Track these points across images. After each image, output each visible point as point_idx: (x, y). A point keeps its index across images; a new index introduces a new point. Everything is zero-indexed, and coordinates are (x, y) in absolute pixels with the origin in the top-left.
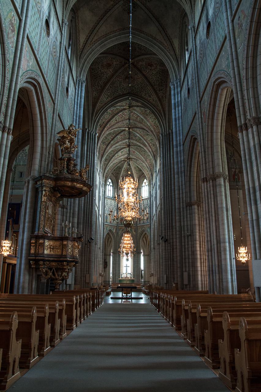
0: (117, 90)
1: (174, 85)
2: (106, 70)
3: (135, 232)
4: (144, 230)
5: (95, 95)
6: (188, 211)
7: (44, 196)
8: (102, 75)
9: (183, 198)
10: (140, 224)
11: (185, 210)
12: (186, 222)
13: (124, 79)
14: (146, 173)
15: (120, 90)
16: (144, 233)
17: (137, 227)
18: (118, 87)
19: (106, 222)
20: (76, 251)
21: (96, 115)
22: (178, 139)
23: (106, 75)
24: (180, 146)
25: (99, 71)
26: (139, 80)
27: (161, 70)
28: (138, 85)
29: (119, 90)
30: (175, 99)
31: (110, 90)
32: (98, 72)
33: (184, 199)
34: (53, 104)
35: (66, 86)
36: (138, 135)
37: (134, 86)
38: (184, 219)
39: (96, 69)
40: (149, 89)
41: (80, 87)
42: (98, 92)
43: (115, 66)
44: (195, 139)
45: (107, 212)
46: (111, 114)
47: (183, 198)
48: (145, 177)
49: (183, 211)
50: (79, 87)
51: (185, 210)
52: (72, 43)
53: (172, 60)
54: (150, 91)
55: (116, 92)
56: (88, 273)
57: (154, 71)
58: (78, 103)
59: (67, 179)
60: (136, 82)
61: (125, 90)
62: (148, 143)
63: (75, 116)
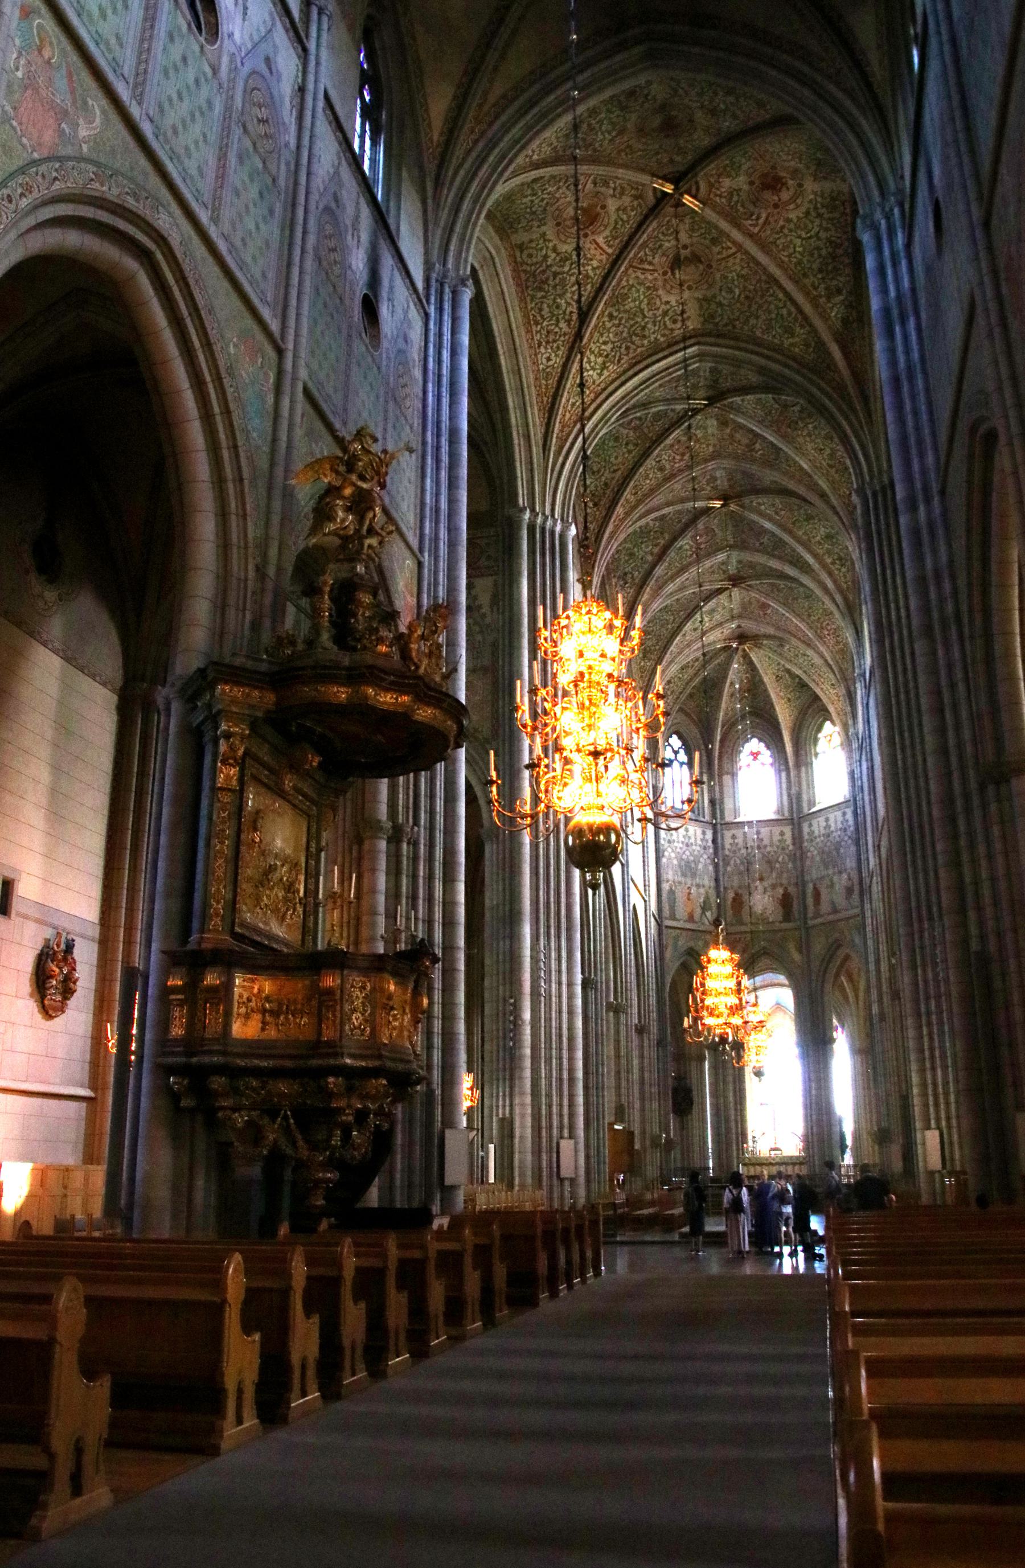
0: (644, 328)
1: (875, 227)
3: (800, 952)
4: (837, 940)
5: (549, 359)
6: (993, 807)
7: (224, 762)
8: (566, 269)
9: (960, 746)
10: (817, 915)
11: (976, 801)
12: (984, 863)
13: (665, 273)
14: (830, 694)
15: (654, 323)
16: (841, 953)
17: (807, 929)
18: (642, 311)
19: (673, 917)
20: (395, 1019)
21: (561, 448)
22: (916, 466)
24: (928, 501)
25: (550, 253)
26: (730, 264)
27: (822, 196)
28: (730, 291)
29: (649, 326)
30: (884, 291)
31: (609, 331)
32: (546, 257)
33: (969, 749)
34: (272, 354)
35: (361, 289)
36: (768, 525)
37: (714, 296)
38: (972, 846)
41: (447, 306)
42: (558, 348)
43: (613, 217)
44: (991, 437)
45: (671, 873)
46: (636, 445)
47: (960, 746)
48: (827, 716)
49: (968, 811)
50: (440, 310)
51: (976, 801)
52: (390, 117)
53: (855, 111)
55: (637, 335)
56: (571, 1137)
57: (792, 206)
58: (440, 376)
59: (328, 674)
60: (718, 276)
61: (675, 322)
62: (815, 556)
63: (429, 434)
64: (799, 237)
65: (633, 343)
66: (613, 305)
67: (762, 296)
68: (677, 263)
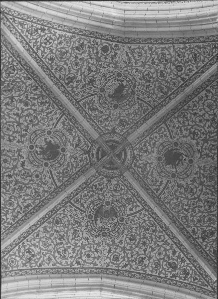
0: (65, 250)
2: (39, 170)
13: (90, 217)
23: (38, 184)
29: (70, 251)
32: (15, 167)
39: (10, 154)
40: (170, 241)
54: (171, 247)
55: (59, 252)
64: (187, 198)
65: (55, 257)
66: (49, 223)
67: (155, 243)
68: (99, 212)
